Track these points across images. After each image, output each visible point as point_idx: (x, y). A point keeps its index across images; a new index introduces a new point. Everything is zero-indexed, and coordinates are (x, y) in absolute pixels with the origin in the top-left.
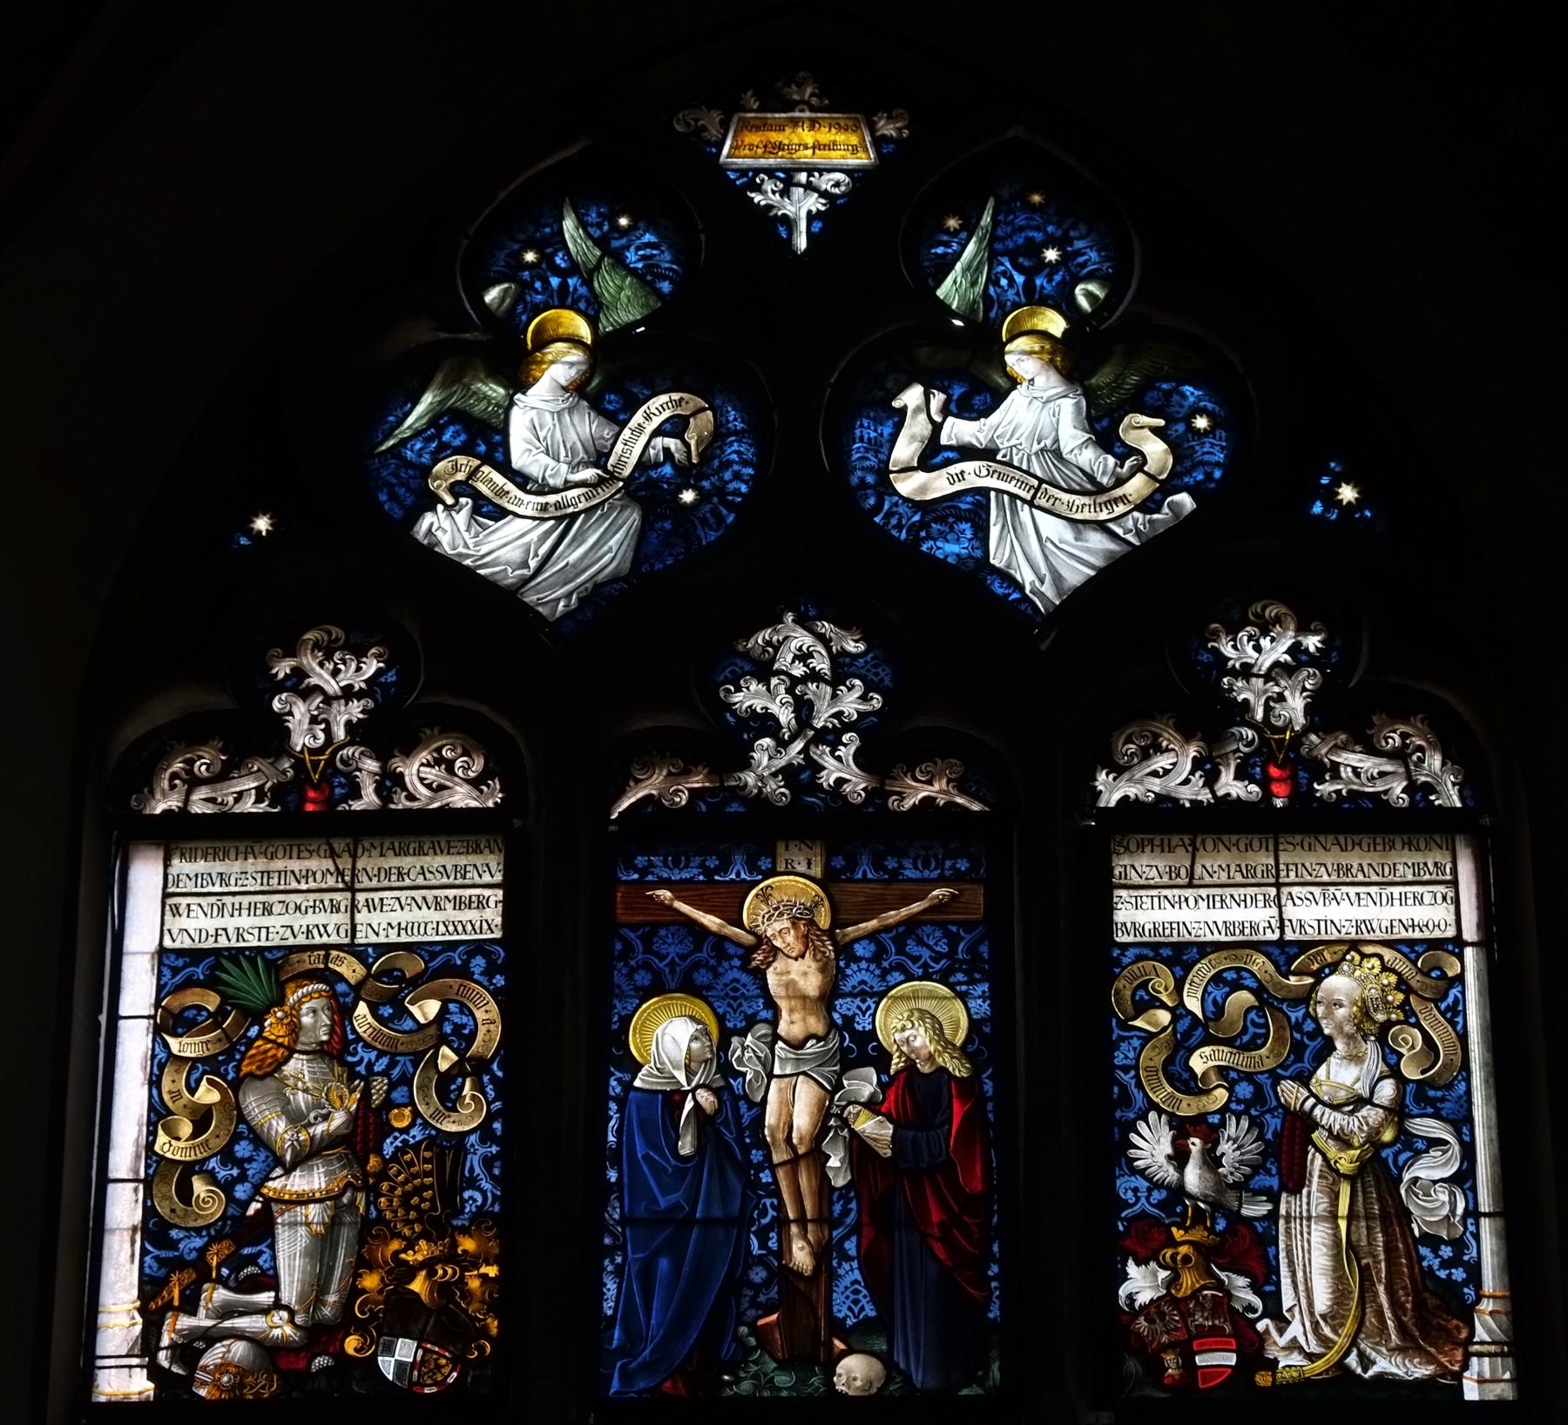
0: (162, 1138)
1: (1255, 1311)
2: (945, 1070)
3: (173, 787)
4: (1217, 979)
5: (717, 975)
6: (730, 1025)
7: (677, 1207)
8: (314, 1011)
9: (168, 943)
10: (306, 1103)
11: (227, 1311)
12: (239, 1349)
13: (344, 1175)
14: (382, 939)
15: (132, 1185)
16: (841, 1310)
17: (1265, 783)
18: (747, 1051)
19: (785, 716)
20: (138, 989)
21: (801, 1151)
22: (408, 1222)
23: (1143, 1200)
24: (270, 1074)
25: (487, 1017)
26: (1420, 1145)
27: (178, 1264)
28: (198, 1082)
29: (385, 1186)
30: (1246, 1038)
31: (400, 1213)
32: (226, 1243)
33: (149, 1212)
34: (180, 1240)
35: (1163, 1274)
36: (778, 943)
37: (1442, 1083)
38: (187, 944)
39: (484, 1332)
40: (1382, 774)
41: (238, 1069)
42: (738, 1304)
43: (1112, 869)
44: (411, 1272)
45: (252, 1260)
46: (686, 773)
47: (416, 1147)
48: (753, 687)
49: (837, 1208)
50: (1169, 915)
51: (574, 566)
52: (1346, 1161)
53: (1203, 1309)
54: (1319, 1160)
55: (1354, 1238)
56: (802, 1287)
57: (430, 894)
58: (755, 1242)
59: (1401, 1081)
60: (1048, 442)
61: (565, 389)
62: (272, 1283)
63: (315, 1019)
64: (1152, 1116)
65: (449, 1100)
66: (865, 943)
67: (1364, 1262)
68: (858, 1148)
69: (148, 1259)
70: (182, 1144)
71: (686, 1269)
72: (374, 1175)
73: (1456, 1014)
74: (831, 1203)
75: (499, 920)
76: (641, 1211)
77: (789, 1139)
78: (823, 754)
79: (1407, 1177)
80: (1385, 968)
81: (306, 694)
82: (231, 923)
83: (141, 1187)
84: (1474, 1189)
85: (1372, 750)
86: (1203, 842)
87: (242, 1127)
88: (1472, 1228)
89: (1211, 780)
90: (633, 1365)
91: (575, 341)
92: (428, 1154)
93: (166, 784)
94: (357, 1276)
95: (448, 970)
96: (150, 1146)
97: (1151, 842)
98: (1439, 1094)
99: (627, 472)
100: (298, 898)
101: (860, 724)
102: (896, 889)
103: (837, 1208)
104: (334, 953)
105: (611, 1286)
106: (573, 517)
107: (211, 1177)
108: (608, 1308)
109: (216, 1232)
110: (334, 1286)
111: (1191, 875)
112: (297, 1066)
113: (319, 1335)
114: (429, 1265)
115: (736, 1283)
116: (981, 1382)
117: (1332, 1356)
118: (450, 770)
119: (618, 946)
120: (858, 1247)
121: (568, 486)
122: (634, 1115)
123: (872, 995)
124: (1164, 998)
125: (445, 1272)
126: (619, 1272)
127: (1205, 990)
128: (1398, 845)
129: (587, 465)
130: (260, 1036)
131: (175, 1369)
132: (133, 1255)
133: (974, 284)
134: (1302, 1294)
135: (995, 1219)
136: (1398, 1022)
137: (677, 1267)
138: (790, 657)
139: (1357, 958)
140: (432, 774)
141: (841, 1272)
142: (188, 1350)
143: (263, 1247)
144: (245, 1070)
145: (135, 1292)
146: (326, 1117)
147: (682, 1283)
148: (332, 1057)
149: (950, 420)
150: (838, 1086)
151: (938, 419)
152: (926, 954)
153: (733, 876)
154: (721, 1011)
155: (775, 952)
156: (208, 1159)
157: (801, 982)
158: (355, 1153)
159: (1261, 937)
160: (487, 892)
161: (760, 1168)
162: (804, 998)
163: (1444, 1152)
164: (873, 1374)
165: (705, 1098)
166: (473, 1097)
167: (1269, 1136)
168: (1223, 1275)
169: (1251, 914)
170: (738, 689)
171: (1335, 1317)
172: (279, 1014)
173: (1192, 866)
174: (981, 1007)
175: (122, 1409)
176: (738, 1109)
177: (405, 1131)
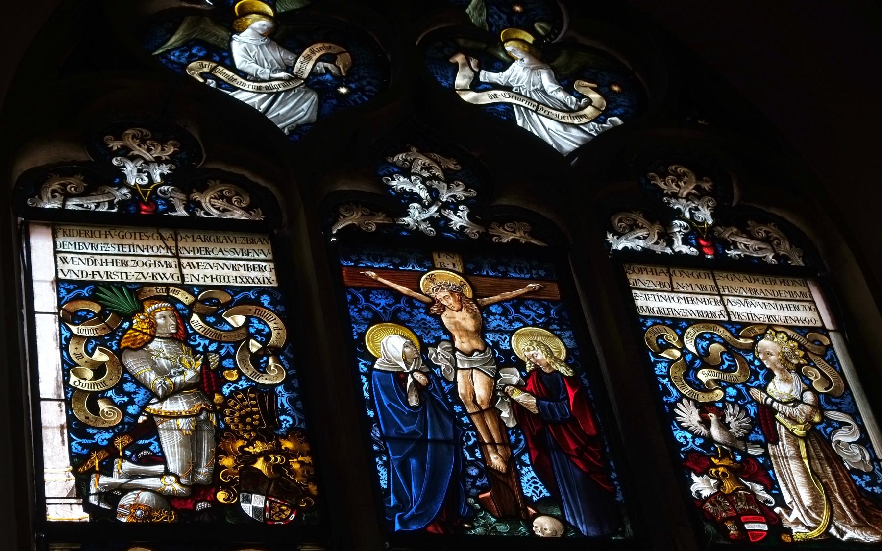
0: (73, 379)
1: (771, 503)
2: (558, 372)
3: (54, 197)
4: (700, 337)
5: (412, 316)
6: (426, 341)
7: (414, 432)
8: (164, 317)
9: (61, 276)
10: (167, 365)
11: (133, 475)
12: (145, 496)
13: (198, 405)
14: (201, 282)
15: (57, 403)
16: (528, 491)
17: (699, 247)
18: (439, 355)
19: (424, 194)
20: (45, 298)
21: (484, 407)
22: (245, 431)
23: (691, 443)
24: (141, 348)
25: (275, 326)
26: (835, 424)
27: (96, 447)
28: (93, 350)
29: (227, 411)
30: (725, 367)
31: (240, 426)
32: (126, 437)
33: (70, 418)
34: (95, 434)
35: (713, 482)
36: (444, 303)
37: (837, 395)
38: (74, 277)
39: (307, 492)
40: (760, 249)
41: (119, 344)
42: (465, 486)
43: (628, 280)
44: (255, 458)
45: (147, 447)
46: (372, 215)
47: (244, 391)
48: (402, 179)
49: (513, 438)
50: (664, 304)
51: (283, 115)
52: (798, 431)
53: (741, 500)
54: (783, 429)
55: (814, 468)
56: (501, 478)
57: (228, 263)
58: (467, 454)
59: (816, 393)
60: (539, 87)
61: (262, 35)
62: (162, 460)
63: (165, 321)
64: (685, 401)
65: (263, 370)
66: (496, 306)
67: (824, 481)
68: (517, 409)
69: (74, 443)
70: (87, 382)
71: (428, 466)
72: (219, 405)
73: (835, 363)
74: (509, 436)
75: (274, 278)
76: (393, 433)
77: (475, 401)
78: (449, 214)
79: (833, 440)
80: (789, 338)
81: (133, 158)
82: (103, 269)
83: (63, 404)
84: (871, 447)
85: (751, 237)
86: (674, 272)
87: (126, 375)
88: (877, 467)
89: (670, 243)
90: (406, 516)
91: (264, 15)
92: (252, 396)
93: (50, 195)
94: (217, 459)
95: (246, 301)
96: (66, 383)
97: (646, 269)
98: (838, 400)
99: (305, 76)
100: (144, 259)
101: (466, 202)
102: (506, 282)
103: (513, 438)
104: (172, 288)
105: (383, 473)
106: (278, 94)
107: (110, 401)
108: (383, 484)
109: (118, 431)
110: (204, 463)
111: (671, 286)
112: (155, 345)
113: (196, 490)
114: (265, 455)
115: (460, 474)
116: (622, 533)
117: (821, 528)
118: (229, 201)
119: (349, 297)
120: (530, 459)
121: (271, 79)
122: (378, 383)
123: (506, 332)
124: (674, 343)
125: (276, 460)
126: (386, 465)
127: (695, 342)
128: (778, 282)
129: (281, 71)
130: (130, 327)
131: (102, 506)
132: (63, 441)
133: (480, 15)
134: (795, 496)
135: (608, 450)
136: (804, 365)
137: (422, 464)
138: (419, 168)
139: (773, 333)
140: (219, 203)
141: (523, 472)
142: (111, 495)
143: (152, 440)
144: (123, 345)
145: (68, 462)
146: (182, 373)
147: (427, 474)
148: (180, 341)
149: (483, 72)
150: (497, 376)
151: (477, 70)
152: (533, 314)
153: (410, 268)
154: (419, 334)
155: (444, 307)
156: (107, 390)
157: (463, 323)
158: (205, 393)
159: (718, 319)
160: (264, 264)
161: (461, 415)
162: (467, 331)
163: (850, 429)
164: (556, 528)
165: (419, 377)
166: (276, 367)
167: (752, 414)
168: (747, 484)
169: (711, 308)
170: (393, 179)
171: (816, 506)
172: (142, 317)
173: (671, 282)
174: (571, 344)
175: (66, 528)
176: (441, 384)
177: (236, 382)
